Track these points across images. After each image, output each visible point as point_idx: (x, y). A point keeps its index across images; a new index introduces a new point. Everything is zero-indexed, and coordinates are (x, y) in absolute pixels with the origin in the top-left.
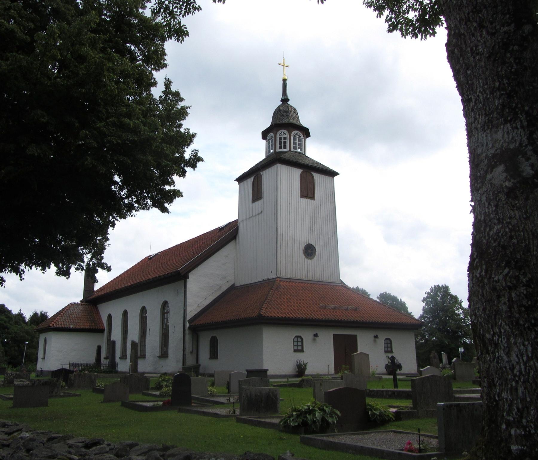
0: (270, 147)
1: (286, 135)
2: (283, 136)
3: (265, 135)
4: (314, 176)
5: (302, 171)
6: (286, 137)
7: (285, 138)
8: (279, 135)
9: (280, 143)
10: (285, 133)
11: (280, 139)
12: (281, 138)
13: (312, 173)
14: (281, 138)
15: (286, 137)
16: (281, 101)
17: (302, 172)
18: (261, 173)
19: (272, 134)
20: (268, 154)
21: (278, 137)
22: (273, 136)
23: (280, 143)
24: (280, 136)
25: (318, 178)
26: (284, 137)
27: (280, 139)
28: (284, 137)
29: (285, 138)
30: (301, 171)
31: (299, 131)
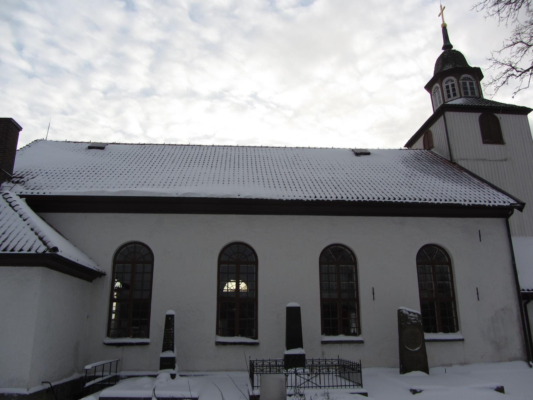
0: (437, 98)
1: (453, 81)
2: (450, 84)
3: (429, 87)
4: (499, 118)
5: (481, 115)
6: (454, 84)
7: (453, 85)
8: (446, 83)
9: (448, 91)
10: (452, 80)
11: (447, 87)
12: (448, 86)
13: (494, 114)
14: (448, 86)
15: (454, 84)
16: (442, 49)
17: (480, 116)
18: (430, 129)
19: (437, 85)
20: (436, 109)
21: (444, 85)
22: (439, 86)
23: (448, 91)
24: (447, 84)
25: (504, 119)
26: (452, 84)
27: (447, 87)
28: (452, 84)
29: (453, 85)
30: (480, 114)
31: (470, 75)
